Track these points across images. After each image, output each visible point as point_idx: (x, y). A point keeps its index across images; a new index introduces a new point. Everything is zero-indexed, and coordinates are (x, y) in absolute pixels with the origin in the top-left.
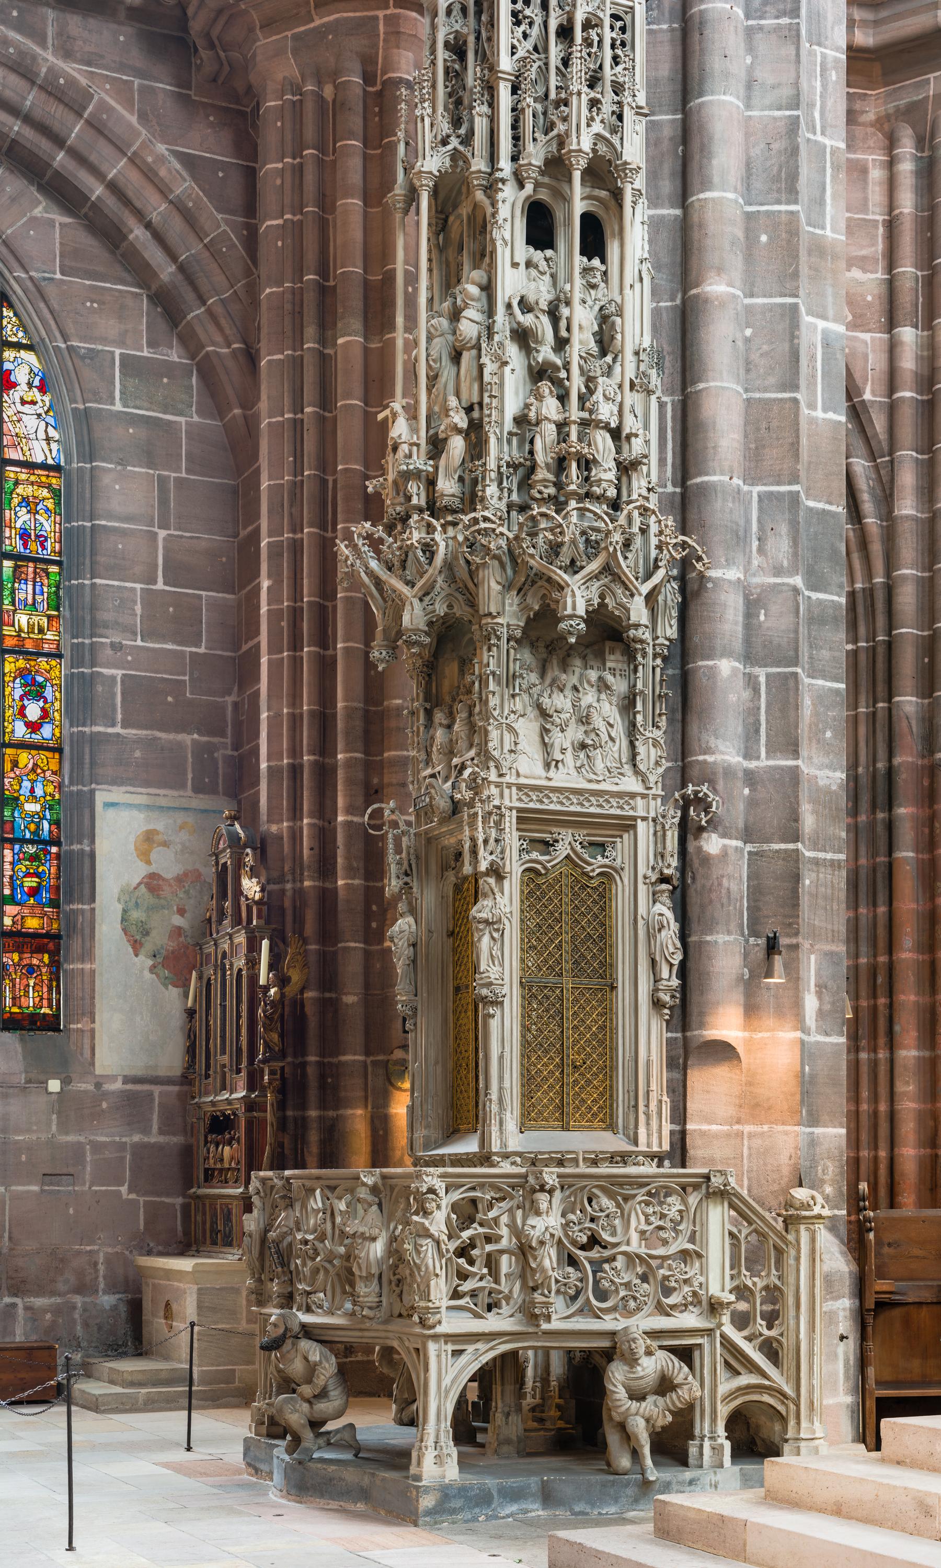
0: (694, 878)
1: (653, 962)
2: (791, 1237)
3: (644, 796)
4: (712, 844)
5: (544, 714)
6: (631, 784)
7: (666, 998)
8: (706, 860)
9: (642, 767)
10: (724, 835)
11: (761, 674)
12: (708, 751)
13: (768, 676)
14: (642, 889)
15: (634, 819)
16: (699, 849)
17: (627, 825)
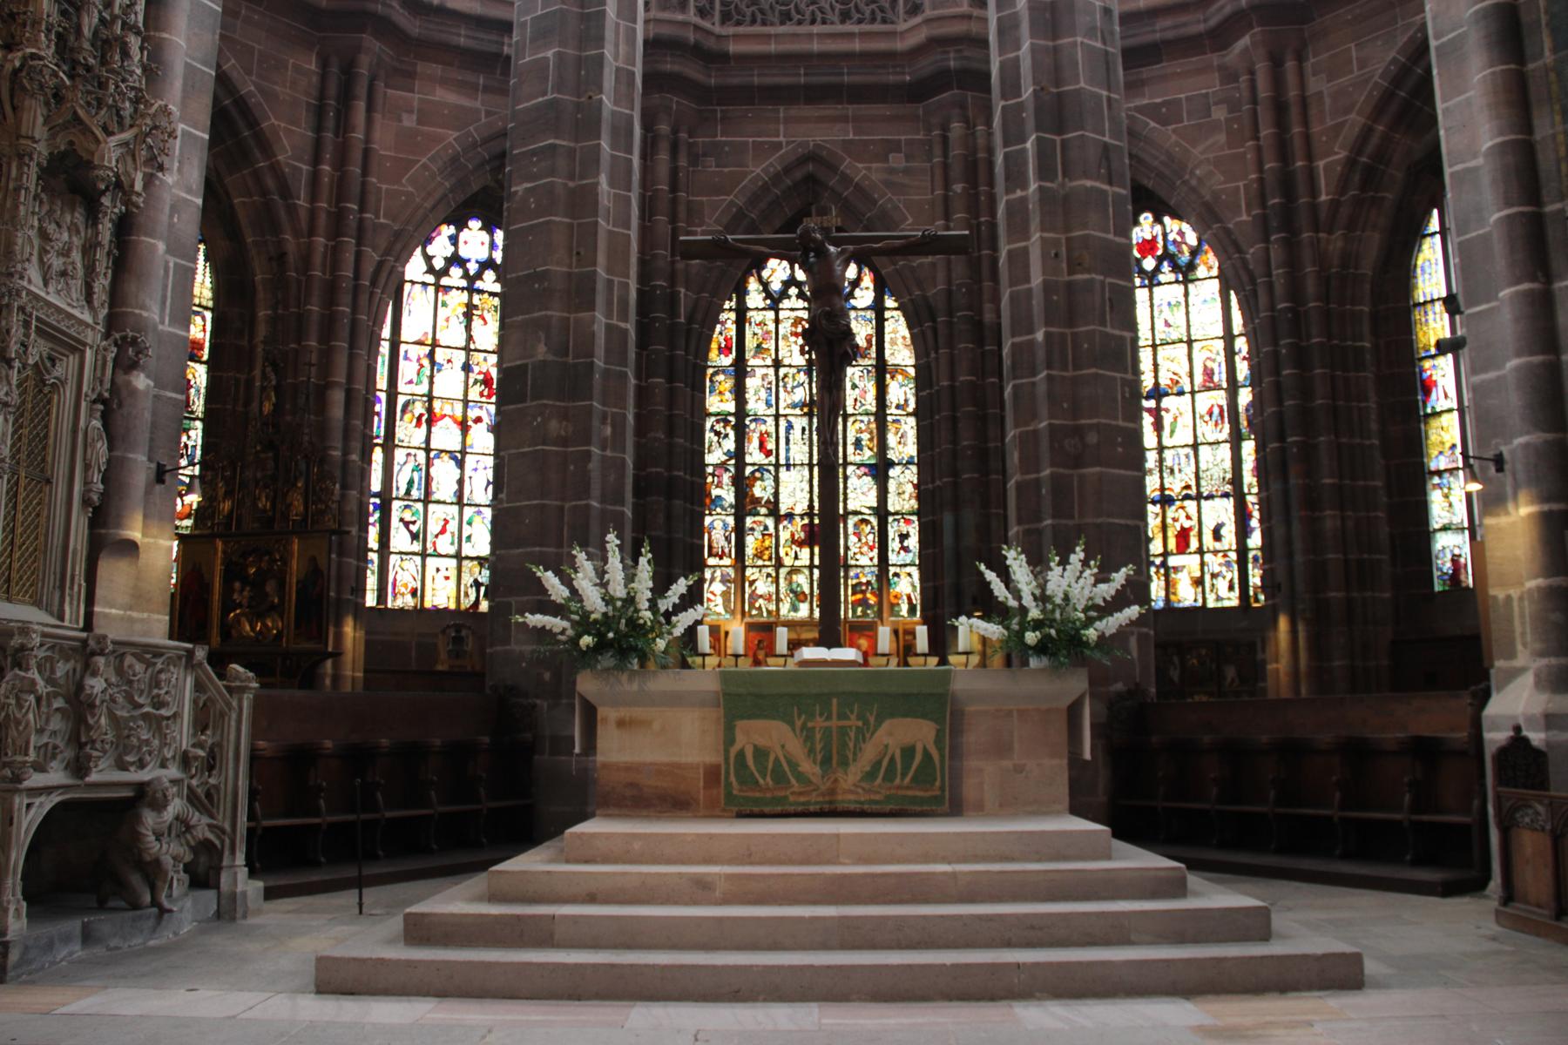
0: (120, 405)
1: (87, 467)
2: (235, 703)
3: (93, 329)
4: (141, 381)
5: (44, 235)
6: (87, 317)
7: (95, 497)
8: (133, 392)
9: (96, 304)
10: (148, 377)
11: (172, 261)
12: (143, 307)
13: (176, 264)
14: (84, 404)
15: (85, 344)
16: (129, 383)
17: (77, 347)
